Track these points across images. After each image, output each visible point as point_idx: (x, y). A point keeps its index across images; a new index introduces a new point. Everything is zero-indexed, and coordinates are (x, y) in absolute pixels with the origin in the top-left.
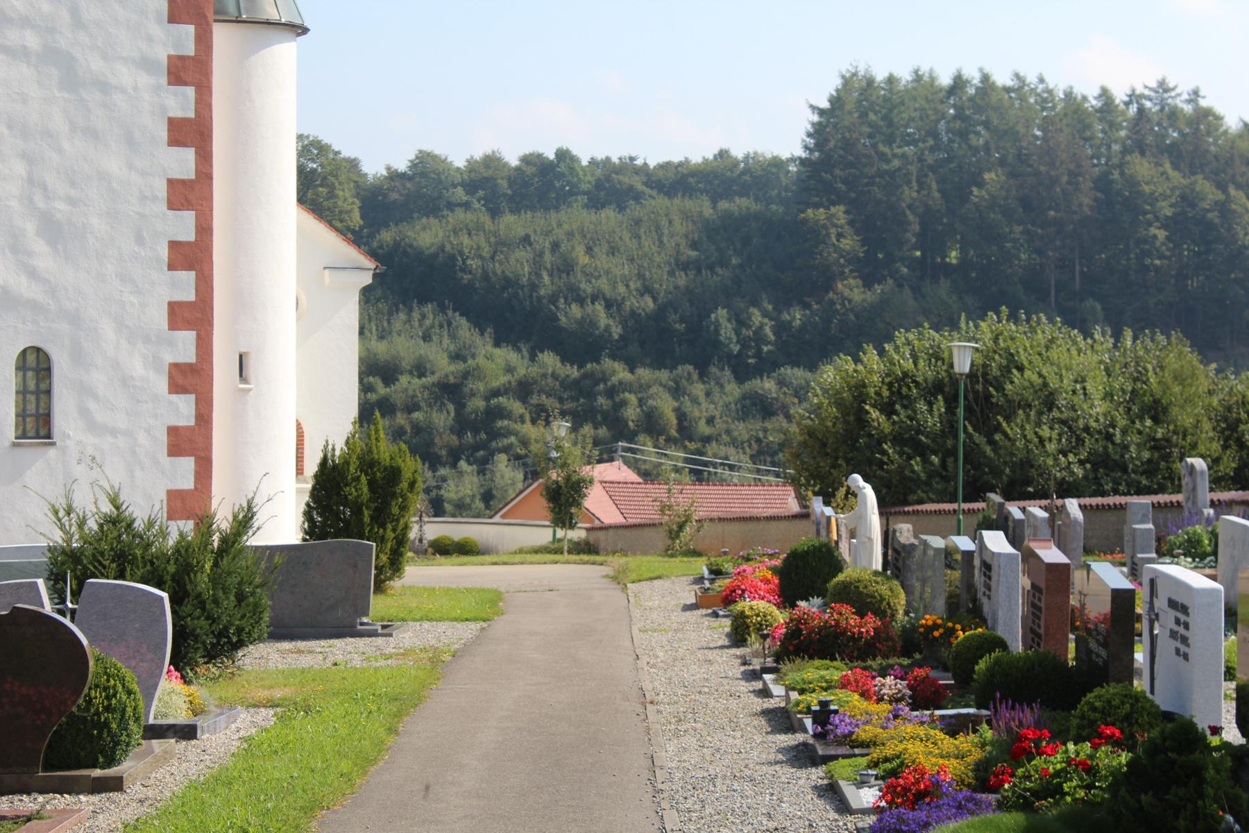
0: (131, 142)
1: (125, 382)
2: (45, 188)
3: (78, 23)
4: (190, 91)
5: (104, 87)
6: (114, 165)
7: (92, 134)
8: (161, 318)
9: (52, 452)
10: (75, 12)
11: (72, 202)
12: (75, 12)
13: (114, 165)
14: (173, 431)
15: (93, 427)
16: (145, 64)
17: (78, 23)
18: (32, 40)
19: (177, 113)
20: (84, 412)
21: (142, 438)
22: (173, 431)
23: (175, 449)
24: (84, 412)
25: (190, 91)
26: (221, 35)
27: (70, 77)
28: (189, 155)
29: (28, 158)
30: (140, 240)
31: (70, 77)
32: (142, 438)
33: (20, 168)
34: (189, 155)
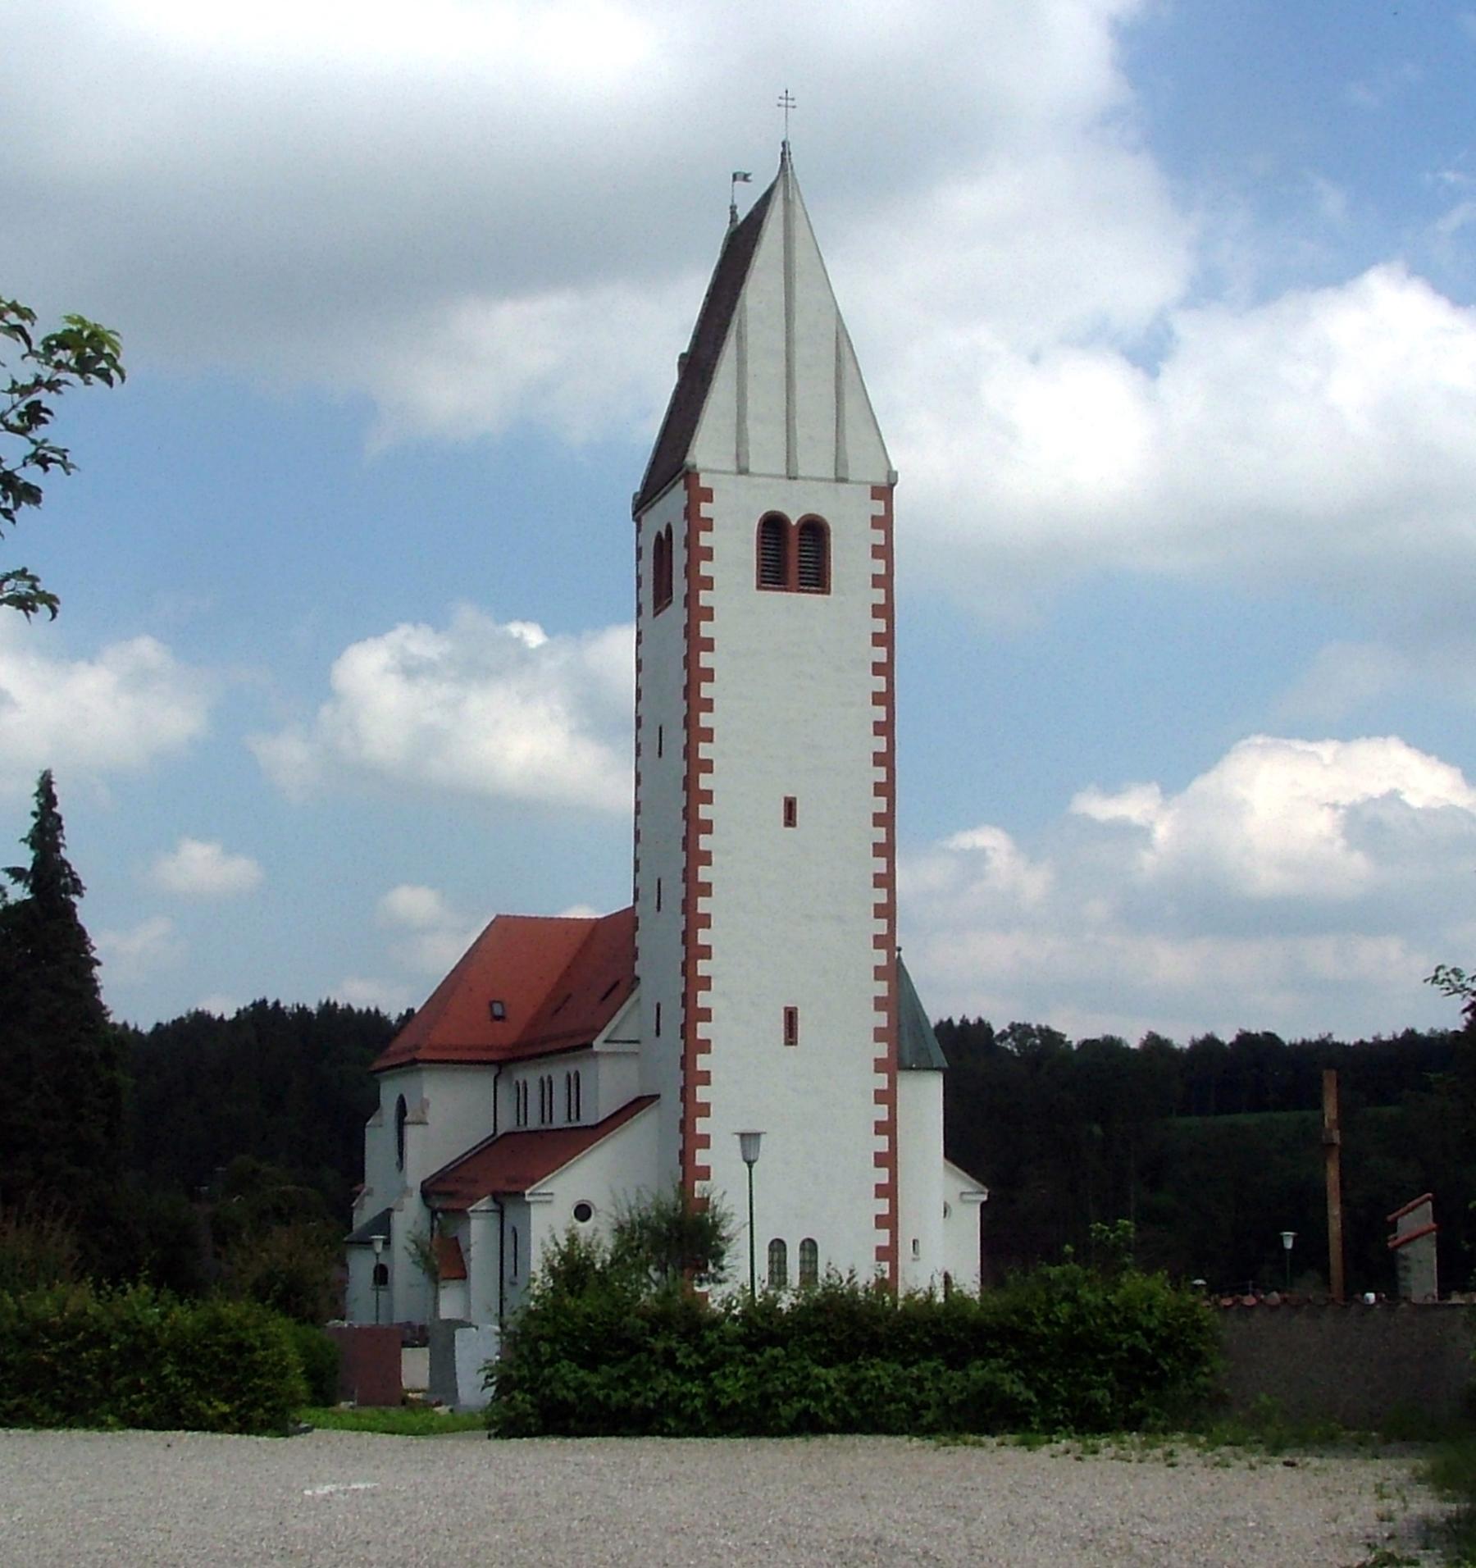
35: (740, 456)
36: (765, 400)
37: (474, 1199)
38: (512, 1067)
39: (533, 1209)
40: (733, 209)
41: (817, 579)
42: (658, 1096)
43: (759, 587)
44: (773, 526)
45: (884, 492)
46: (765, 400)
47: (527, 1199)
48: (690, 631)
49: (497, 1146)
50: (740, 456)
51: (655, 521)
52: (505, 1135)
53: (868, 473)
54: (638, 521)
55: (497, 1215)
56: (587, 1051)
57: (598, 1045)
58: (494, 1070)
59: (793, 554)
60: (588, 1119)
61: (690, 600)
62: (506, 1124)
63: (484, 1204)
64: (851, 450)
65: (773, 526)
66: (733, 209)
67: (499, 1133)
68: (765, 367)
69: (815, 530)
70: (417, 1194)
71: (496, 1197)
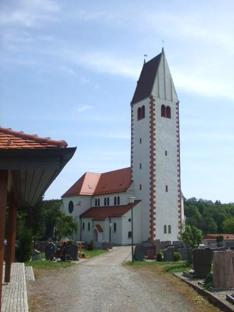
35: (159, 95)
36: (162, 87)
37: (106, 218)
41: (169, 116)
44: (163, 107)
45: (177, 104)
46: (162, 87)
48: (151, 122)
49: (91, 209)
50: (159, 95)
51: (139, 105)
53: (175, 101)
54: (132, 107)
57: (128, 191)
59: (166, 112)
60: (121, 204)
61: (151, 117)
62: (93, 205)
63: (108, 218)
64: (174, 98)
65: (163, 107)
68: (161, 82)
69: (169, 108)
70: (79, 218)
71: (109, 217)
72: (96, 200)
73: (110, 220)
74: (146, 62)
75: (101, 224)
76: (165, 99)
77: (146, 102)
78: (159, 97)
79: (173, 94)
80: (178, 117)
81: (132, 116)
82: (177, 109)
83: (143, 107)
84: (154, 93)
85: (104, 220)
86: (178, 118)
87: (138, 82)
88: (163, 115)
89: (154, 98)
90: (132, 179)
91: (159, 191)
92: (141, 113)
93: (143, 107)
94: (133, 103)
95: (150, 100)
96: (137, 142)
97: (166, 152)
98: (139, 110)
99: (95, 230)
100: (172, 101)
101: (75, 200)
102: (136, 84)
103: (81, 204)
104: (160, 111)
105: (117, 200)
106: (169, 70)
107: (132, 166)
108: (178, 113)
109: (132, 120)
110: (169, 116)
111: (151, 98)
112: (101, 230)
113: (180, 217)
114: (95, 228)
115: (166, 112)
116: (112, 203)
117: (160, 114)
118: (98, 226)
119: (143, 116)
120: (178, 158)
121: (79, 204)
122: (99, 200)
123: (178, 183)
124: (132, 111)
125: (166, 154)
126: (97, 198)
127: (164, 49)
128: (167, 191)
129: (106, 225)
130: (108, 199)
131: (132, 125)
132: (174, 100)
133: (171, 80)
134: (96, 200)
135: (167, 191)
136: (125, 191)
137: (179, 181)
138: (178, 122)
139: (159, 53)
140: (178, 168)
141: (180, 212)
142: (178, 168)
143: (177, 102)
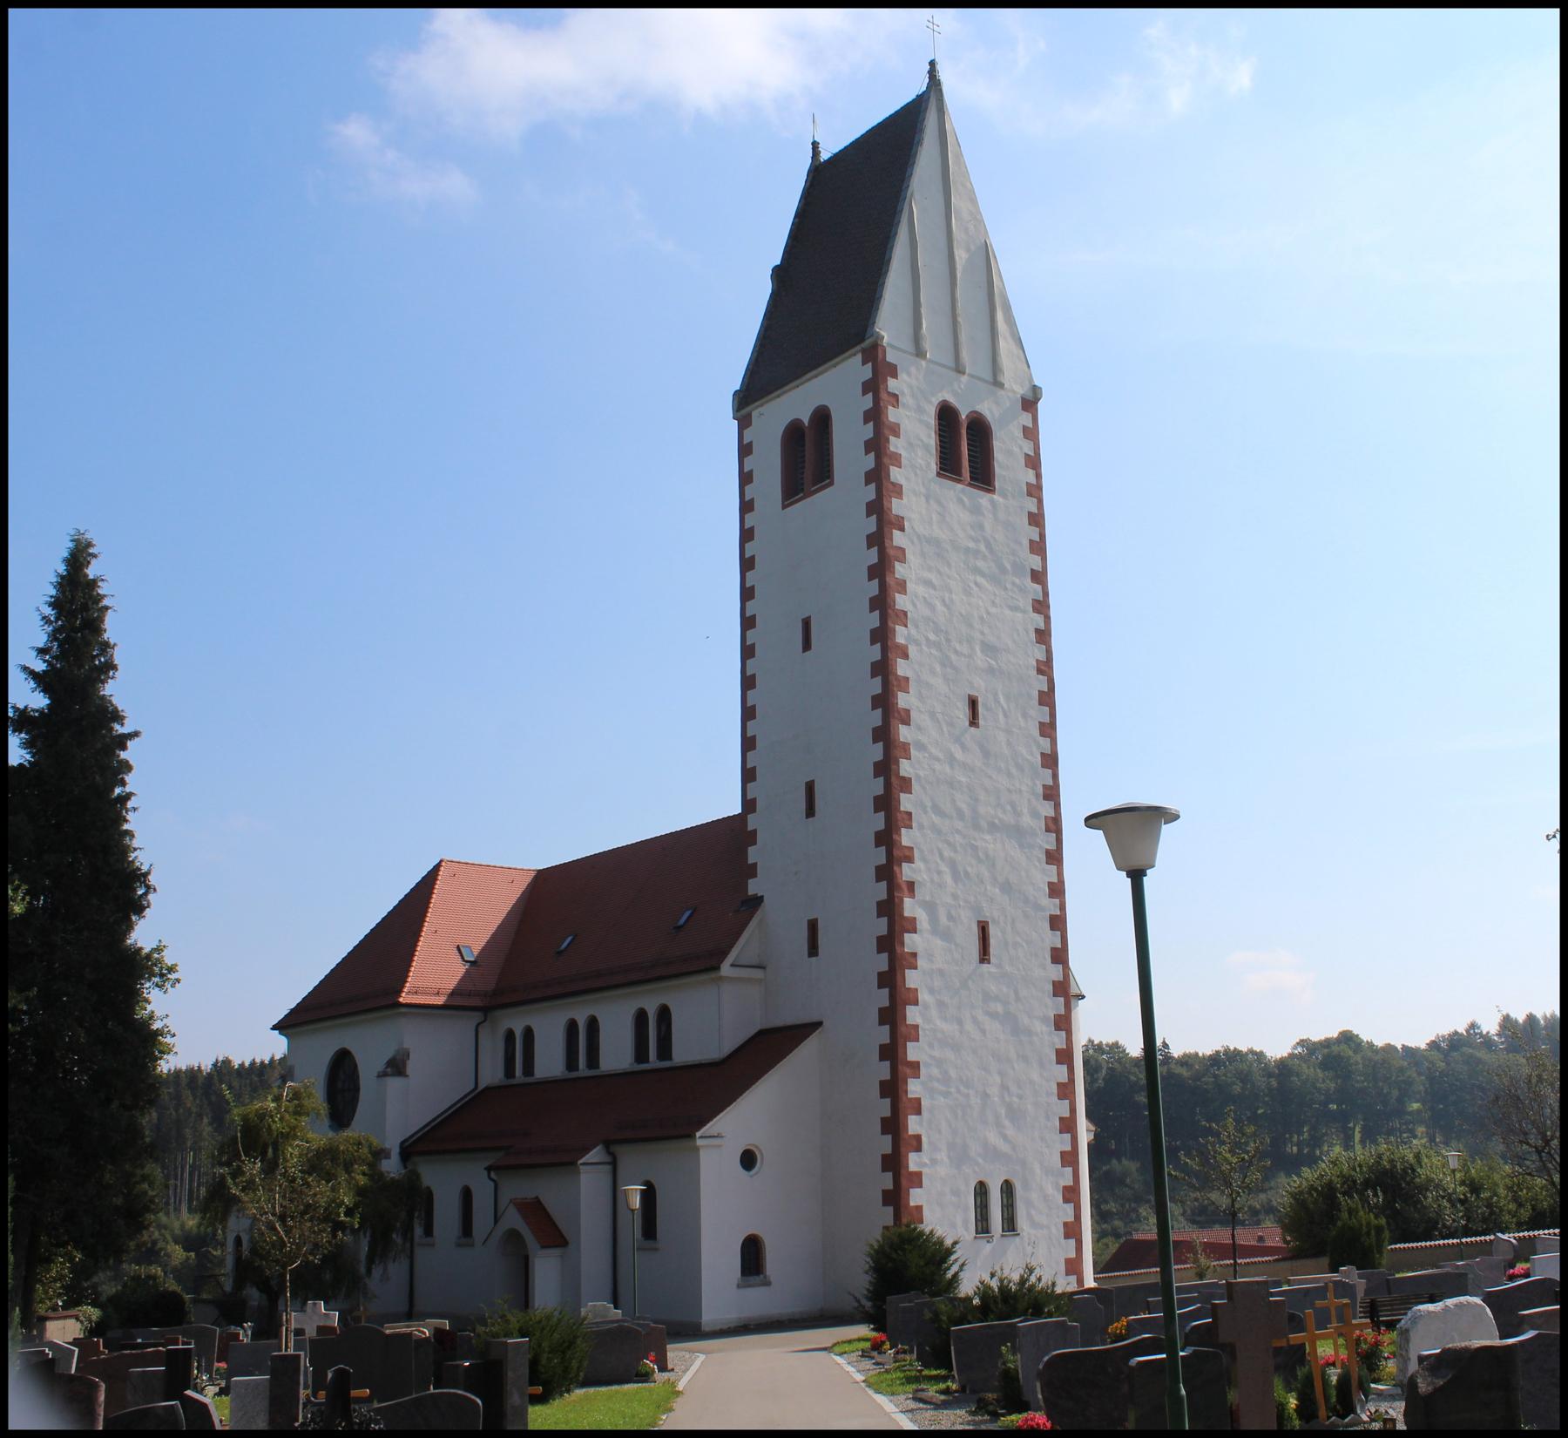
0: (1042, 1065)
1: (1045, 1198)
2: (1008, 1089)
3: (1018, 999)
4: (1063, 1033)
5: (1029, 1033)
6: (1035, 1076)
7: (1025, 1059)
8: (1056, 1160)
9: (1017, 1239)
10: (1016, 993)
11: (1020, 1097)
12: (1016, 993)
13: (1035, 1076)
14: (1065, 1224)
15: (1034, 1225)
16: (1044, 1019)
17: (1018, 999)
18: (999, 1008)
19: (1059, 1046)
20: (1030, 1217)
21: (1054, 1230)
22: (1065, 1224)
23: (1067, 1236)
24: (1030, 1217)
25: (1063, 1033)
26: (1073, 1001)
27: (1016, 1029)
28: (1064, 1068)
29: (1000, 1073)
30: (1048, 1118)
31: (1016, 1029)
32: (1054, 1230)
33: (998, 1079)
34: (1064, 1068)
37: (586, 1150)
38: (498, 1013)
39: (703, 1154)
40: (815, 145)
41: (983, 477)
42: (820, 1024)
43: (939, 475)
44: (946, 415)
45: (1030, 404)
47: (699, 1142)
49: (477, 1102)
51: (795, 403)
52: (487, 1089)
53: (1015, 388)
54: (744, 422)
55: (608, 1168)
56: (713, 975)
57: (726, 969)
58: (477, 1017)
62: (492, 1073)
64: (1005, 360)
66: (815, 145)
67: (481, 1087)
69: (980, 430)
71: (608, 1144)
72: (510, 1036)
73: (614, 1164)
74: (825, 156)
75: (548, 1190)
76: (959, 369)
77: (835, 387)
78: (920, 353)
79: (1005, 345)
80: (1039, 487)
81: (745, 478)
82: (1031, 433)
83: (822, 418)
84: (889, 325)
85: (573, 1163)
86: (1035, 491)
87: (778, 274)
88: (948, 465)
89: (891, 357)
90: (754, 887)
91: (934, 951)
92: (805, 459)
93: (822, 418)
94: (747, 399)
95: (867, 372)
96: (778, 634)
97: (973, 703)
98: (794, 436)
99: (513, 1236)
100: (998, 384)
101: (369, 1043)
102: (765, 289)
103: (410, 1067)
104: (930, 439)
105: (654, 1031)
106: (973, 200)
107: (749, 805)
108: (1034, 462)
109: (746, 507)
110: (983, 477)
111: (873, 354)
112: (554, 1237)
113: (1068, 1126)
114: (513, 1219)
115: (966, 449)
116: (616, 1053)
117: (934, 467)
118: (535, 1211)
119: (824, 474)
120: (1045, 743)
121: (396, 1066)
122: (529, 1034)
123: (1052, 906)
124: (745, 450)
125: (974, 721)
126: (516, 1022)
127: (938, 67)
128: (984, 955)
129: (588, 1194)
130: (593, 1024)
131: (746, 535)
132: (1007, 378)
133: (986, 256)
134: (510, 1036)
135: (984, 955)
136: (706, 962)
137: (1057, 890)
138: (1037, 519)
139: (909, 96)
140: (1047, 809)
141: (1066, 1091)
142: (1047, 809)
143: (1030, 396)
